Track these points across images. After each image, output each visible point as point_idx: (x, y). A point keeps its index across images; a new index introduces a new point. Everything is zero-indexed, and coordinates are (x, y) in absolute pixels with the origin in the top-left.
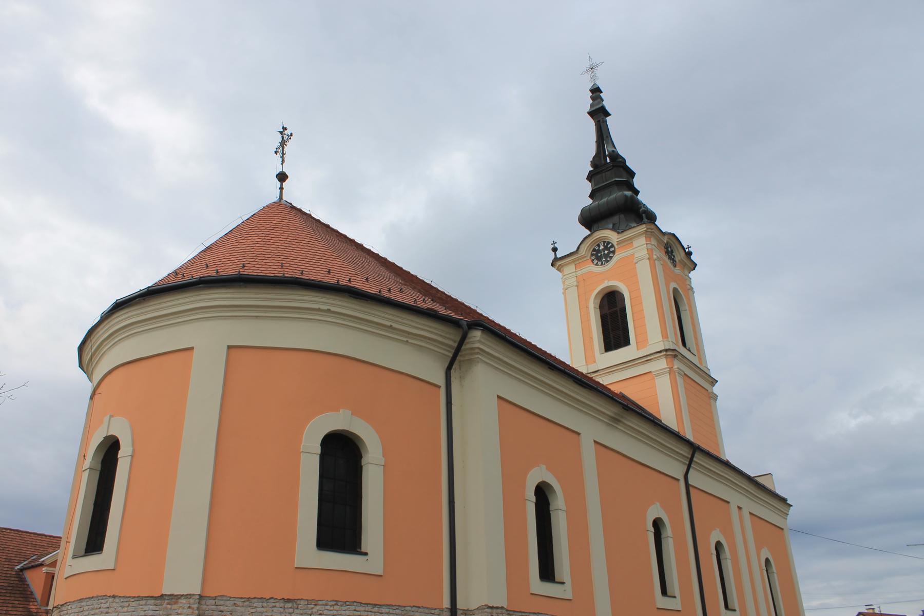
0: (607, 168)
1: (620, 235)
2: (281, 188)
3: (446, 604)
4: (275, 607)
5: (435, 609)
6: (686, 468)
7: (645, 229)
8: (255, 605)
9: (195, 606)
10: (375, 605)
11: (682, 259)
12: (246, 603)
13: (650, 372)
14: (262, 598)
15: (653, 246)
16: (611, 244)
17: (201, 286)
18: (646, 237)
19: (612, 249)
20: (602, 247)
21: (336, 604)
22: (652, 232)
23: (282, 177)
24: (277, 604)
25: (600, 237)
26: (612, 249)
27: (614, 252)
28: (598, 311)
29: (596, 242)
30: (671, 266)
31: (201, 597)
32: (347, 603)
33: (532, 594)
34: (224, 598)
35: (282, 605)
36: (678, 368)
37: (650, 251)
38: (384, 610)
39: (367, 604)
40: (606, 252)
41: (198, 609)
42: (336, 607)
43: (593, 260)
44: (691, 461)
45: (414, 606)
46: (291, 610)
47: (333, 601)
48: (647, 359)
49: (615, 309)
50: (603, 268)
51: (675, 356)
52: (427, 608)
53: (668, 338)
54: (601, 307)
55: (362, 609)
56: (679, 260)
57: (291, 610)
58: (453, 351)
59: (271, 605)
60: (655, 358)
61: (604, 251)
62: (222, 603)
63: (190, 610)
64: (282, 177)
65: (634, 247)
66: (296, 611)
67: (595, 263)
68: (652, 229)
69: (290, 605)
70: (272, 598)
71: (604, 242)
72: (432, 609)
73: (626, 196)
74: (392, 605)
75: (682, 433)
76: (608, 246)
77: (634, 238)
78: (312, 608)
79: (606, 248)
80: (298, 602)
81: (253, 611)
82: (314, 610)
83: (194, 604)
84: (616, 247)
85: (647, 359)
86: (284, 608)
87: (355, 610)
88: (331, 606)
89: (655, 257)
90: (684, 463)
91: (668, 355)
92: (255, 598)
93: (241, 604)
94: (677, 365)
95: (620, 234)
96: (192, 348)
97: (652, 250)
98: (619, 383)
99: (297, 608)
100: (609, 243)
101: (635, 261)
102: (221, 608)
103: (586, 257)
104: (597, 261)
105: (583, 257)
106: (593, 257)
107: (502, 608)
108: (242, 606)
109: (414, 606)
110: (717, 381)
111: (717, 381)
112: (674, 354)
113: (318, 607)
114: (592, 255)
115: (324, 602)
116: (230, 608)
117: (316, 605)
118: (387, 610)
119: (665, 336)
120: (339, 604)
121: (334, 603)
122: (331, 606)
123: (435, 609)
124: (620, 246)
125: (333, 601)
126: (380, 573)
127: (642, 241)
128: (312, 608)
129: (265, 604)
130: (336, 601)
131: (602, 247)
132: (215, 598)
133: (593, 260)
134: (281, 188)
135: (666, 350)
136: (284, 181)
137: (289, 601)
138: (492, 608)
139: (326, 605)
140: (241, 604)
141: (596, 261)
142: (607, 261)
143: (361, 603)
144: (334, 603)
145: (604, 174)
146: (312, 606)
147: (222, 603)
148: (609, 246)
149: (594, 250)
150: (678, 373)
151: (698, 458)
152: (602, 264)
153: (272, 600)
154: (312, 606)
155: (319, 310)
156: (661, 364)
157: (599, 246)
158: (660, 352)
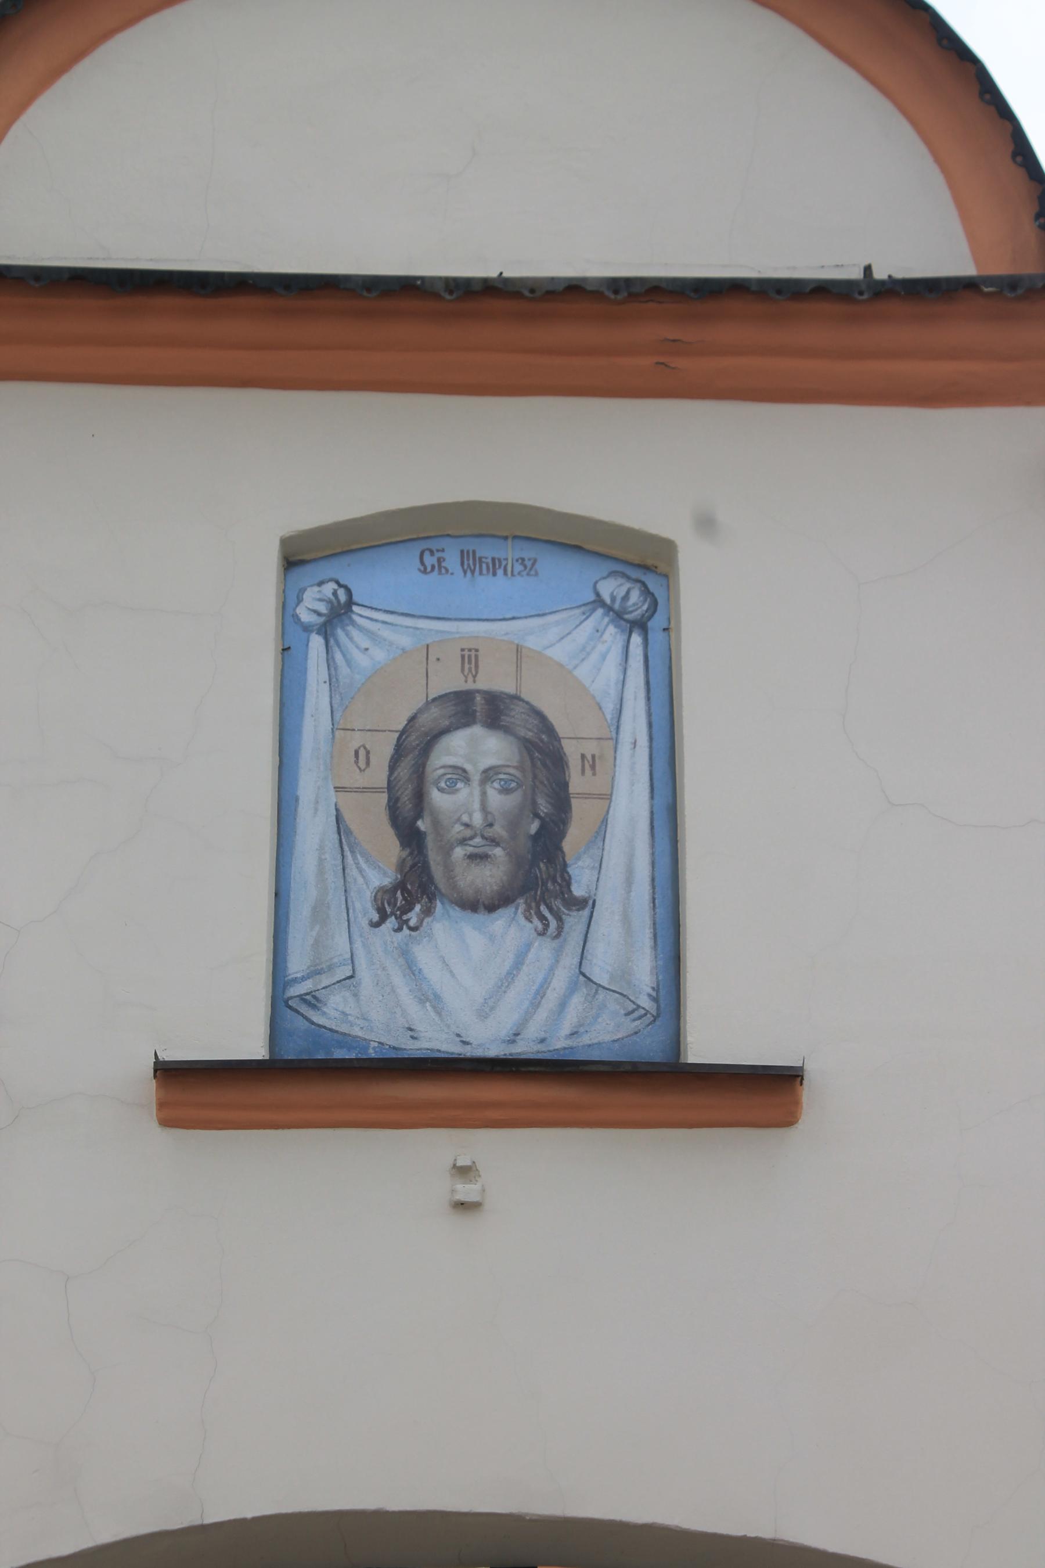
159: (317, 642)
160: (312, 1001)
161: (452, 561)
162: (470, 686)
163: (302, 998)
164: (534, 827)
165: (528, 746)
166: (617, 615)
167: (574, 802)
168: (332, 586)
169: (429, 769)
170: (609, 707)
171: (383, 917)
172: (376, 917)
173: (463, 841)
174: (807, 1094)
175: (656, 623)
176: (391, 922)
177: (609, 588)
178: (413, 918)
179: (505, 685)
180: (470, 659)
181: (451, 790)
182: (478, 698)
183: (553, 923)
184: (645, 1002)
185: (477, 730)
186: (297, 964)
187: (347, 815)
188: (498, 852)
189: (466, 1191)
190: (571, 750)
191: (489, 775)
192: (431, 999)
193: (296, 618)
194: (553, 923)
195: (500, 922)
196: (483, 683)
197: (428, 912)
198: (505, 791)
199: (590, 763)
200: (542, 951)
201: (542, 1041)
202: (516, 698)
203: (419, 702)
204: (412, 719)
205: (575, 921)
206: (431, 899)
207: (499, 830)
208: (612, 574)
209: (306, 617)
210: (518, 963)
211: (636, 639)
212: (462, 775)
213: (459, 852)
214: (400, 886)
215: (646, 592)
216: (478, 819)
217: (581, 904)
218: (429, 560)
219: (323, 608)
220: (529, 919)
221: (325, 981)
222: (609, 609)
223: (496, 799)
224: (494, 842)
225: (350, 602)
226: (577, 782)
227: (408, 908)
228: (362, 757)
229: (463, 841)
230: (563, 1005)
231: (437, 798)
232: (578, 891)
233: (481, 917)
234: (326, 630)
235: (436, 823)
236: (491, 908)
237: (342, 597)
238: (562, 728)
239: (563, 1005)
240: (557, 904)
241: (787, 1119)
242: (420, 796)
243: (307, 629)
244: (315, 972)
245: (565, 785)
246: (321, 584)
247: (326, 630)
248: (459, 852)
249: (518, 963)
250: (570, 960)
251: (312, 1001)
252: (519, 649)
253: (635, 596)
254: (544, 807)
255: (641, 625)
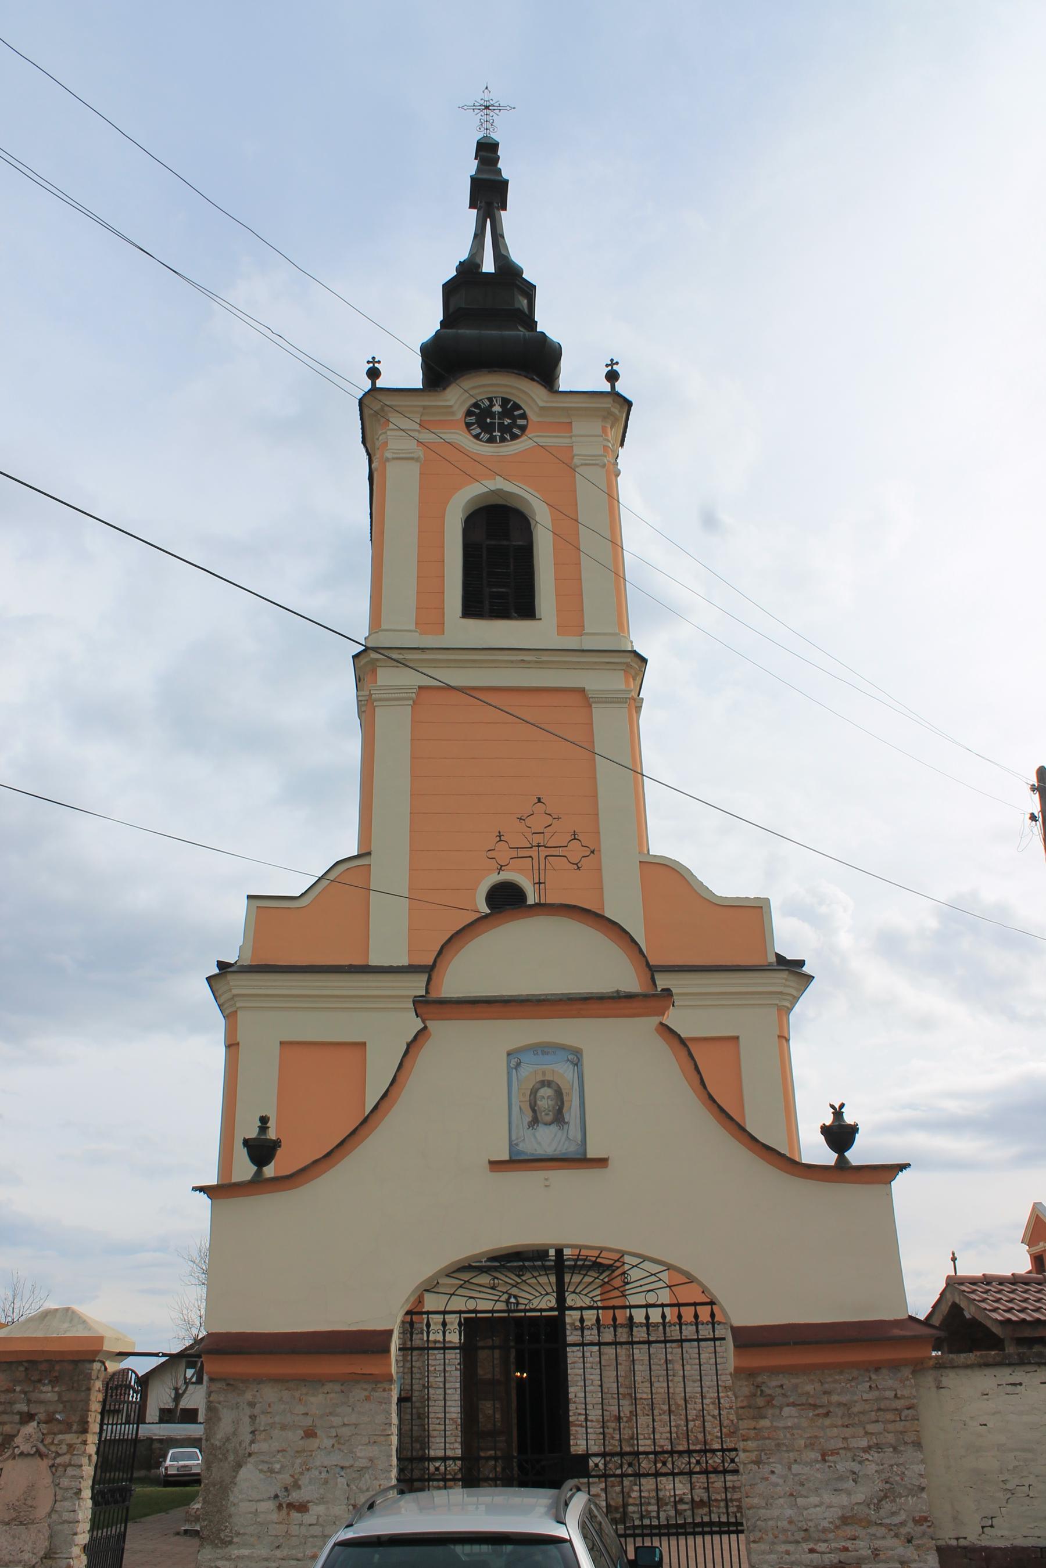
76: (511, 409)
159: (514, 1070)
160: (517, 1145)
161: (540, 1052)
162: (544, 1079)
163: (515, 1144)
164: (557, 1108)
165: (556, 1091)
166: (572, 1062)
167: (565, 1102)
168: (516, 1059)
169: (537, 1096)
170: (571, 1082)
171: (529, 1127)
172: (528, 1127)
173: (544, 1111)
174: (610, 1162)
175: (579, 1064)
176: (531, 1128)
177: (570, 1057)
178: (535, 1127)
179: (551, 1079)
180: (544, 1073)
181: (541, 1101)
182: (546, 1081)
183: (562, 1127)
184: (579, 1143)
185: (546, 1088)
186: (514, 1138)
187: (522, 1107)
188: (551, 1113)
189: (547, 1183)
190: (564, 1092)
191: (548, 1097)
192: (539, 1143)
193: (510, 1066)
194: (562, 1127)
195: (552, 1126)
196: (547, 1078)
197: (538, 1126)
198: (551, 1100)
199: (568, 1094)
200: (560, 1132)
201: (560, 1151)
202: (552, 1081)
203: (534, 1083)
204: (533, 1087)
205: (566, 1126)
206: (538, 1123)
207: (551, 1108)
208: (571, 1054)
209: (512, 1066)
210: (555, 1136)
211: (576, 1067)
212: (543, 1098)
213: (543, 1113)
214: (533, 1121)
215: (577, 1057)
216: (546, 1107)
217: (567, 1123)
218: (535, 1053)
219: (514, 1063)
220: (557, 1126)
221: (519, 1140)
222: (571, 1061)
223: (550, 1103)
224: (550, 1111)
225: (520, 1062)
226: (565, 1098)
227: (534, 1125)
228: (524, 1094)
229: (544, 1111)
230: (564, 1143)
231: (539, 1102)
232: (566, 1120)
233: (548, 1126)
234: (516, 1068)
235: (539, 1108)
236: (550, 1125)
237: (519, 1061)
238: (562, 1087)
239: (564, 1143)
240: (562, 1123)
241: (606, 1166)
242: (535, 1102)
243: (512, 1068)
244: (517, 1139)
245: (563, 1099)
246: (515, 1058)
247: (516, 1068)
248: (543, 1113)
249: (555, 1136)
250: (565, 1133)
251: (517, 1145)
252: (553, 1071)
253: (575, 1058)
254: (559, 1104)
255: (576, 1064)
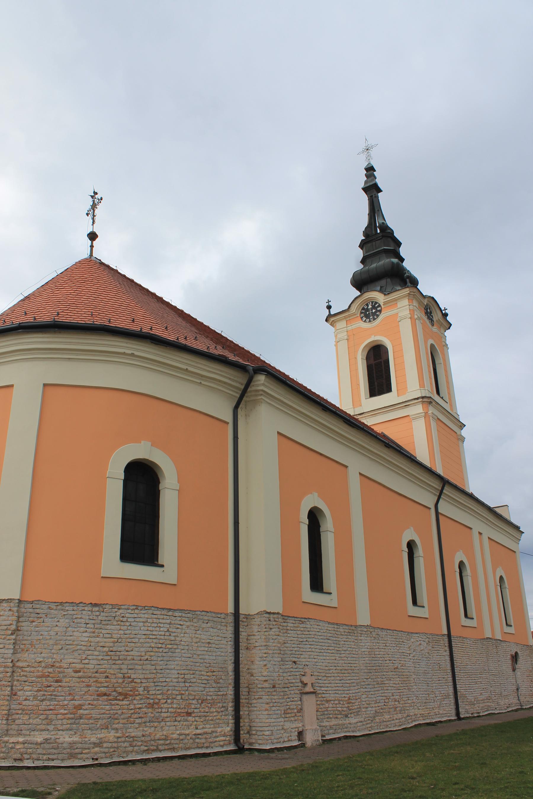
0: (377, 238)
1: (387, 297)
2: (92, 246)
3: (231, 609)
4: (84, 610)
5: (221, 614)
6: (436, 498)
7: (409, 292)
8: (67, 608)
9: (16, 609)
10: (170, 610)
11: (439, 319)
12: (59, 607)
13: (408, 416)
14: (72, 603)
15: (415, 308)
16: (378, 304)
17: (20, 331)
18: (409, 299)
19: (379, 309)
20: (370, 307)
21: (136, 609)
22: (414, 295)
23: (93, 236)
24: (86, 608)
25: (369, 298)
26: (379, 309)
27: (380, 311)
28: (365, 361)
29: (366, 301)
30: (430, 326)
31: (20, 601)
32: (146, 608)
33: (303, 602)
34: (40, 603)
35: (90, 608)
36: (432, 413)
37: (412, 312)
38: (177, 614)
39: (163, 609)
40: (374, 311)
41: (18, 611)
42: (136, 611)
43: (362, 318)
44: (441, 492)
45: (203, 611)
46: (98, 613)
47: (134, 605)
48: (406, 404)
49: (380, 360)
50: (370, 325)
51: (430, 403)
52: (214, 613)
53: (424, 387)
54: (368, 358)
55: (158, 612)
56: (437, 321)
57: (98, 613)
58: (240, 392)
59: (81, 608)
60: (413, 404)
61: (372, 310)
62: (38, 606)
63: (11, 613)
64: (93, 236)
65: (399, 307)
66: (102, 614)
67: (364, 320)
68: (414, 293)
69: (96, 609)
70: (81, 603)
71: (372, 302)
72: (218, 613)
73: (393, 263)
74: (184, 610)
75: (433, 469)
76: (376, 306)
77: (399, 299)
78: (116, 612)
79: (374, 307)
80: (104, 606)
81: (65, 613)
82: (117, 613)
83: (14, 607)
84: (383, 307)
85: (406, 404)
86: (92, 611)
87: (153, 614)
88: (132, 610)
89: (416, 317)
90: (435, 495)
91: (424, 402)
92: (66, 603)
93: (55, 608)
94: (431, 410)
95: (386, 296)
96: (12, 386)
97: (413, 310)
98: (381, 424)
99: (103, 612)
100: (376, 303)
101: (399, 319)
102: (38, 611)
103: (356, 314)
104: (365, 319)
105: (354, 314)
106: (362, 315)
107: (278, 613)
108: (56, 610)
109: (203, 611)
110: (465, 426)
111: (465, 426)
112: (429, 401)
113: (121, 611)
114: (361, 313)
115: (126, 607)
116: (46, 611)
117: (119, 609)
118: (180, 614)
119: (422, 385)
120: (139, 608)
121: (135, 607)
122: (132, 610)
123: (221, 614)
124: (385, 306)
125: (134, 605)
126: (175, 583)
127: (405, 302)
128: (116, 612)
129: (75, 608)
130: (136, 606)
131: (370, 307)
132: (32, 602)
133: (362, 318)
134: (92, 246)
135: (423, 398)
136: (94, 240)
137: (96, 605)
138: (269, 613)
139: (128, 609)
140: (55, 608)
141: (364, 319)
142: (374, 319)
143: (158, 608)
144: (135, 607)
145: (374, 243)
146: (116, 610)
147: (38, 606)
148: (376, 306)
149: (363, 309)
150: (432, 417)
151: (447, 490)
152: (370, 321)
153: (81, 605)
154: (116, 610)
155: (124, 354)
156: (418, 409)
157: (367, 305)
158: (417, 399)
